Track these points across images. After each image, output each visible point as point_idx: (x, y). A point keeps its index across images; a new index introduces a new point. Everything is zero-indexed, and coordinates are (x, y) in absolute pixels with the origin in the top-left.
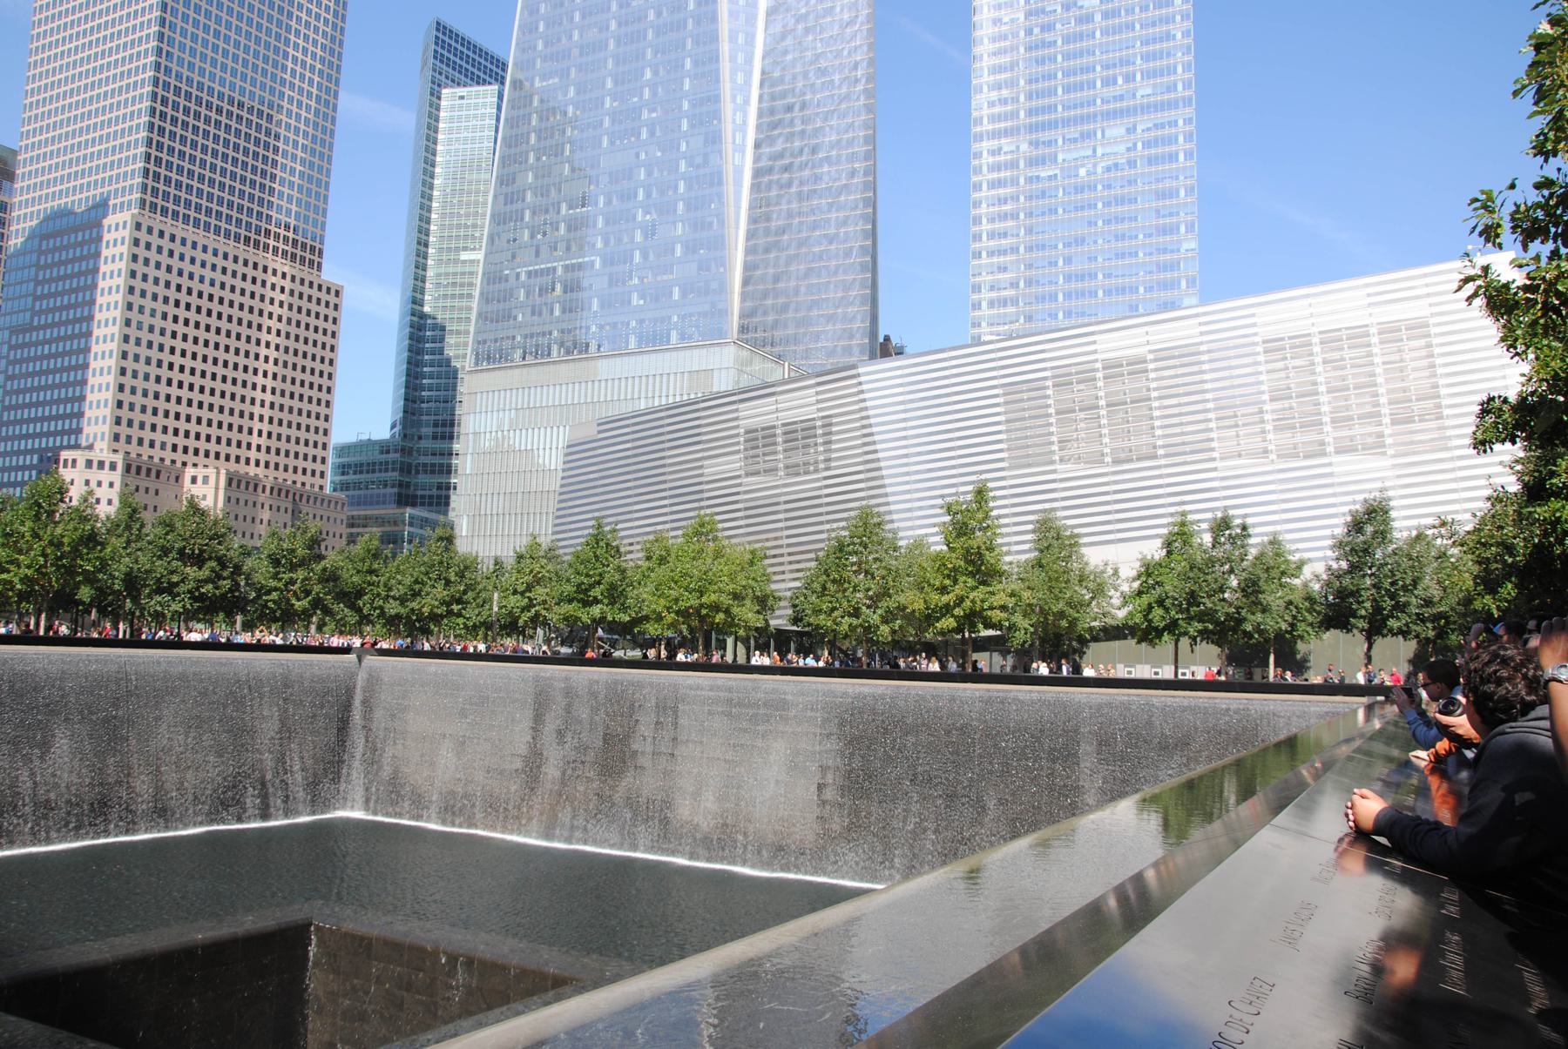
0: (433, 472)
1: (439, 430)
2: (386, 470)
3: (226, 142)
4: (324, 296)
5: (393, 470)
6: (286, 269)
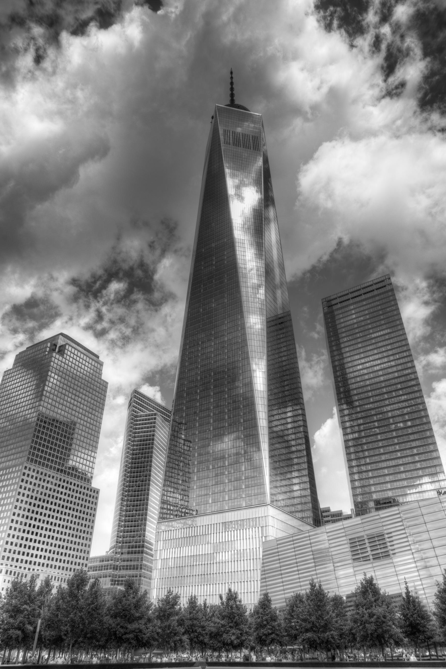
0: (127, 569)
1: (130, 550)
2: (107, 569)
3: (62, 435)
4: (92, 493)
5: (110, 569)
6: (79, 483)
